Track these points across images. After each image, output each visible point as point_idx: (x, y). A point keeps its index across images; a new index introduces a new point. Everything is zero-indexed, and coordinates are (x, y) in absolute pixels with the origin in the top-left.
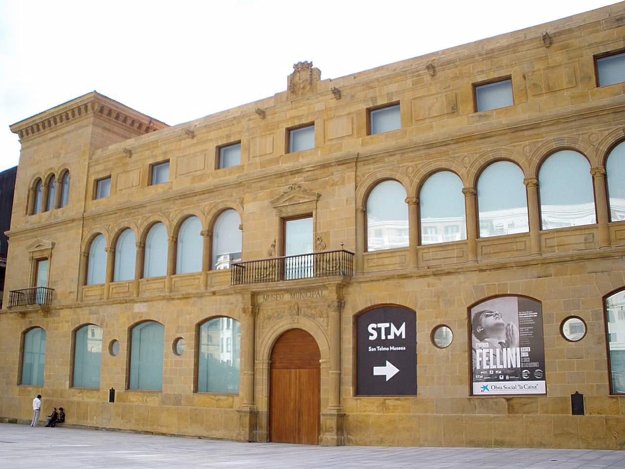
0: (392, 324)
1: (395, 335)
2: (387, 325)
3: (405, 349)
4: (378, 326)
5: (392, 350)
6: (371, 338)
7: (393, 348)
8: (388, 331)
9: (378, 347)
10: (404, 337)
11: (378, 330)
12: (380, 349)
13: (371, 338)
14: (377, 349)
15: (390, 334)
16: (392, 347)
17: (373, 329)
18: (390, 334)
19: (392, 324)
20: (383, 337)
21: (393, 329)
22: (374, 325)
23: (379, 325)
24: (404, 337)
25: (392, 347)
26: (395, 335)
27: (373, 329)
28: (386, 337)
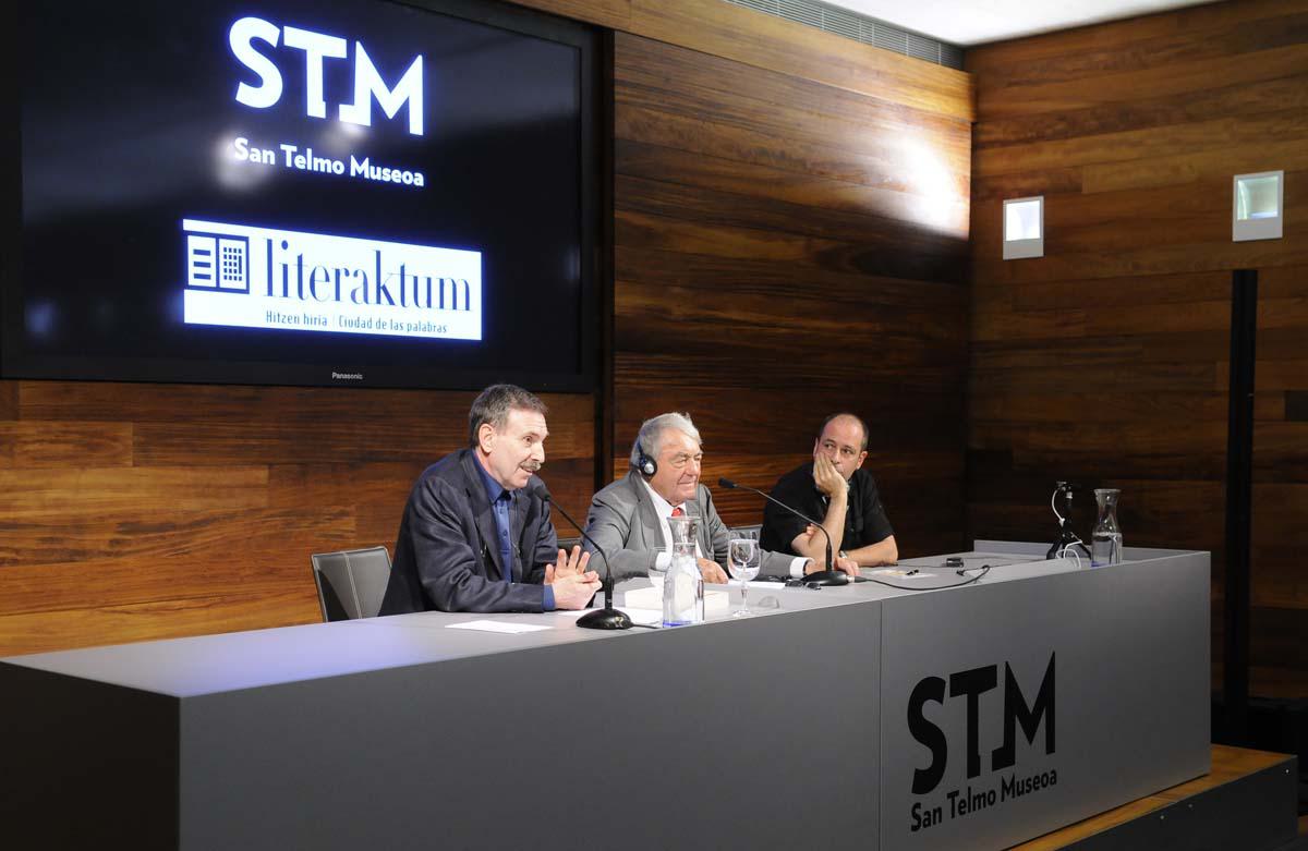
0: (359, 47)
1: (376, 108)
2: (336, 47)
3: (419, 180)
4: (288, 43)
5: (360, 177)
6: (246, 95)
7: (365, 169)
8: (339, 80)
9: (289, 149)
10: (416, 127)
11: (290, 62)
12: (300, 162)
13: (246, 95)
14: (281, 156)
15: (349, 100)
16: (360, 162)
17: (258, 44)
18: (349, 100)
19: (359, 47)
20: (316, 107)
21: (366, 74)
22: (268, 32)
23: (296, 37)
24: (416, 127)
25: (360, 162)
26: (376, 108)
27: (258, 44)
28: (332, 109)
